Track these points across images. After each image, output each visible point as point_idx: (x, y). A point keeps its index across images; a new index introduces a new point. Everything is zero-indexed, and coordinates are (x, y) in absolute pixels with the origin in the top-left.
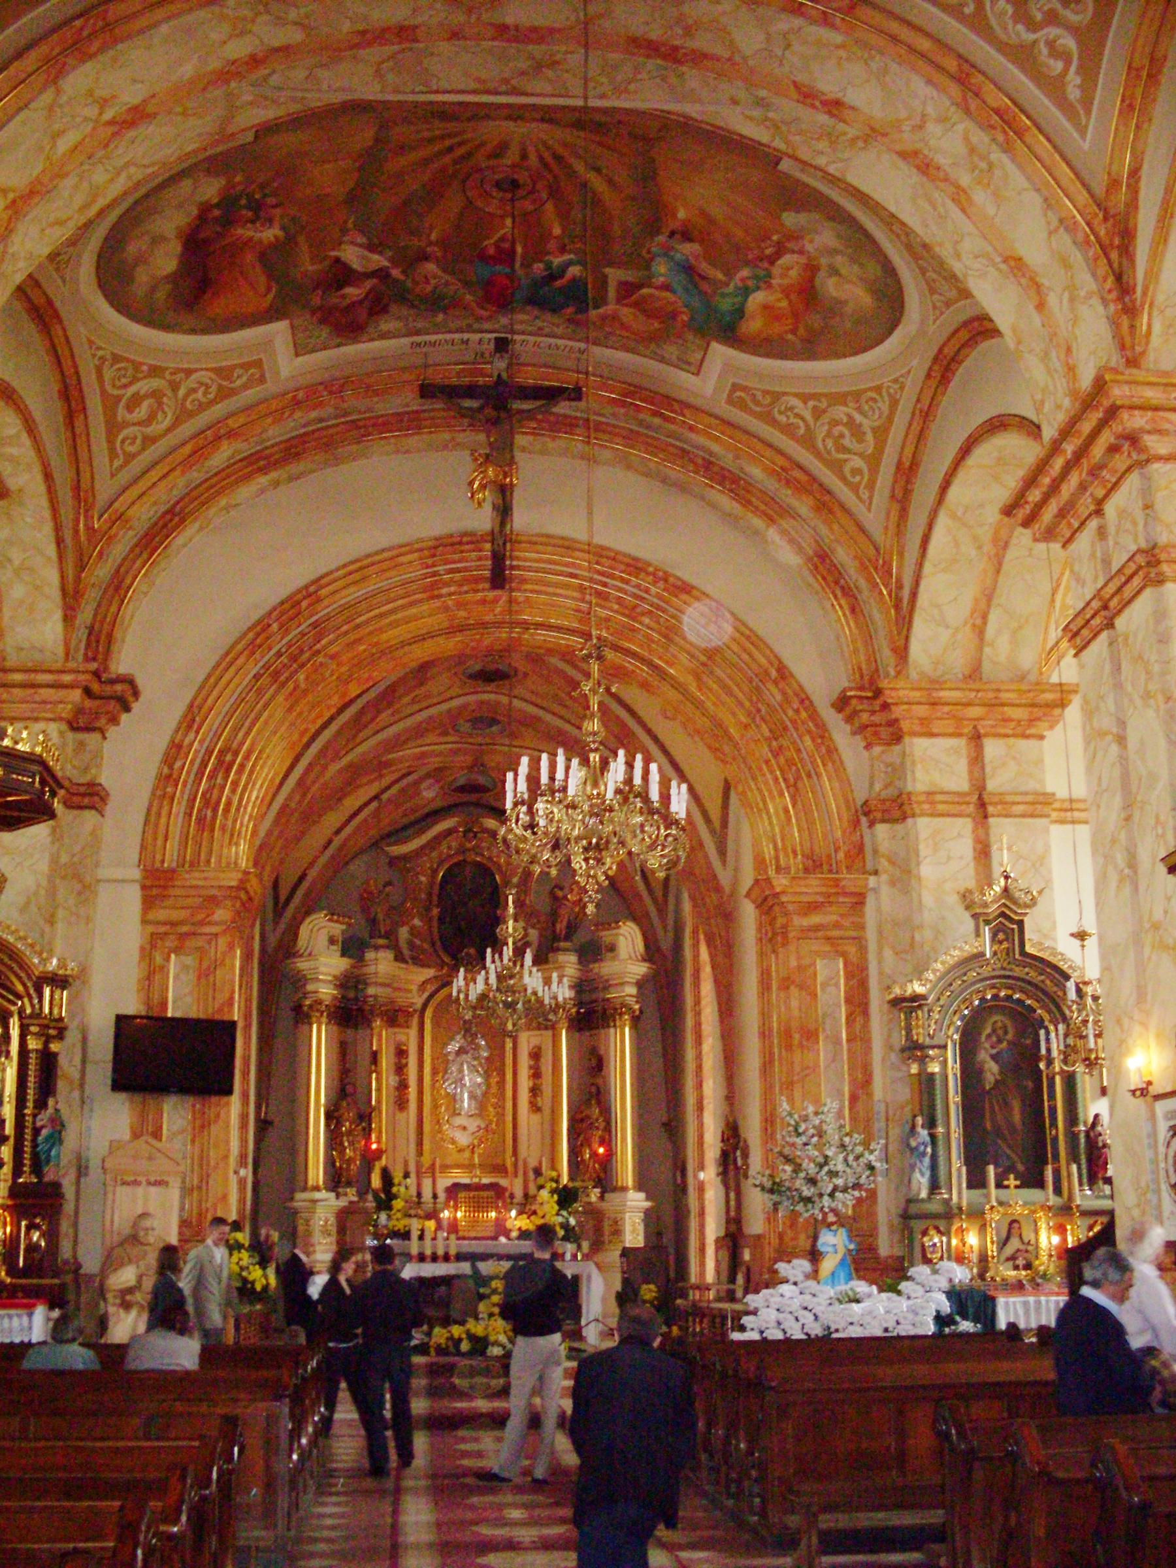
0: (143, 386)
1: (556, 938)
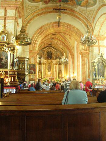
0: (29, 8)
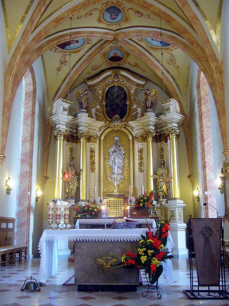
1: (147, 108)
